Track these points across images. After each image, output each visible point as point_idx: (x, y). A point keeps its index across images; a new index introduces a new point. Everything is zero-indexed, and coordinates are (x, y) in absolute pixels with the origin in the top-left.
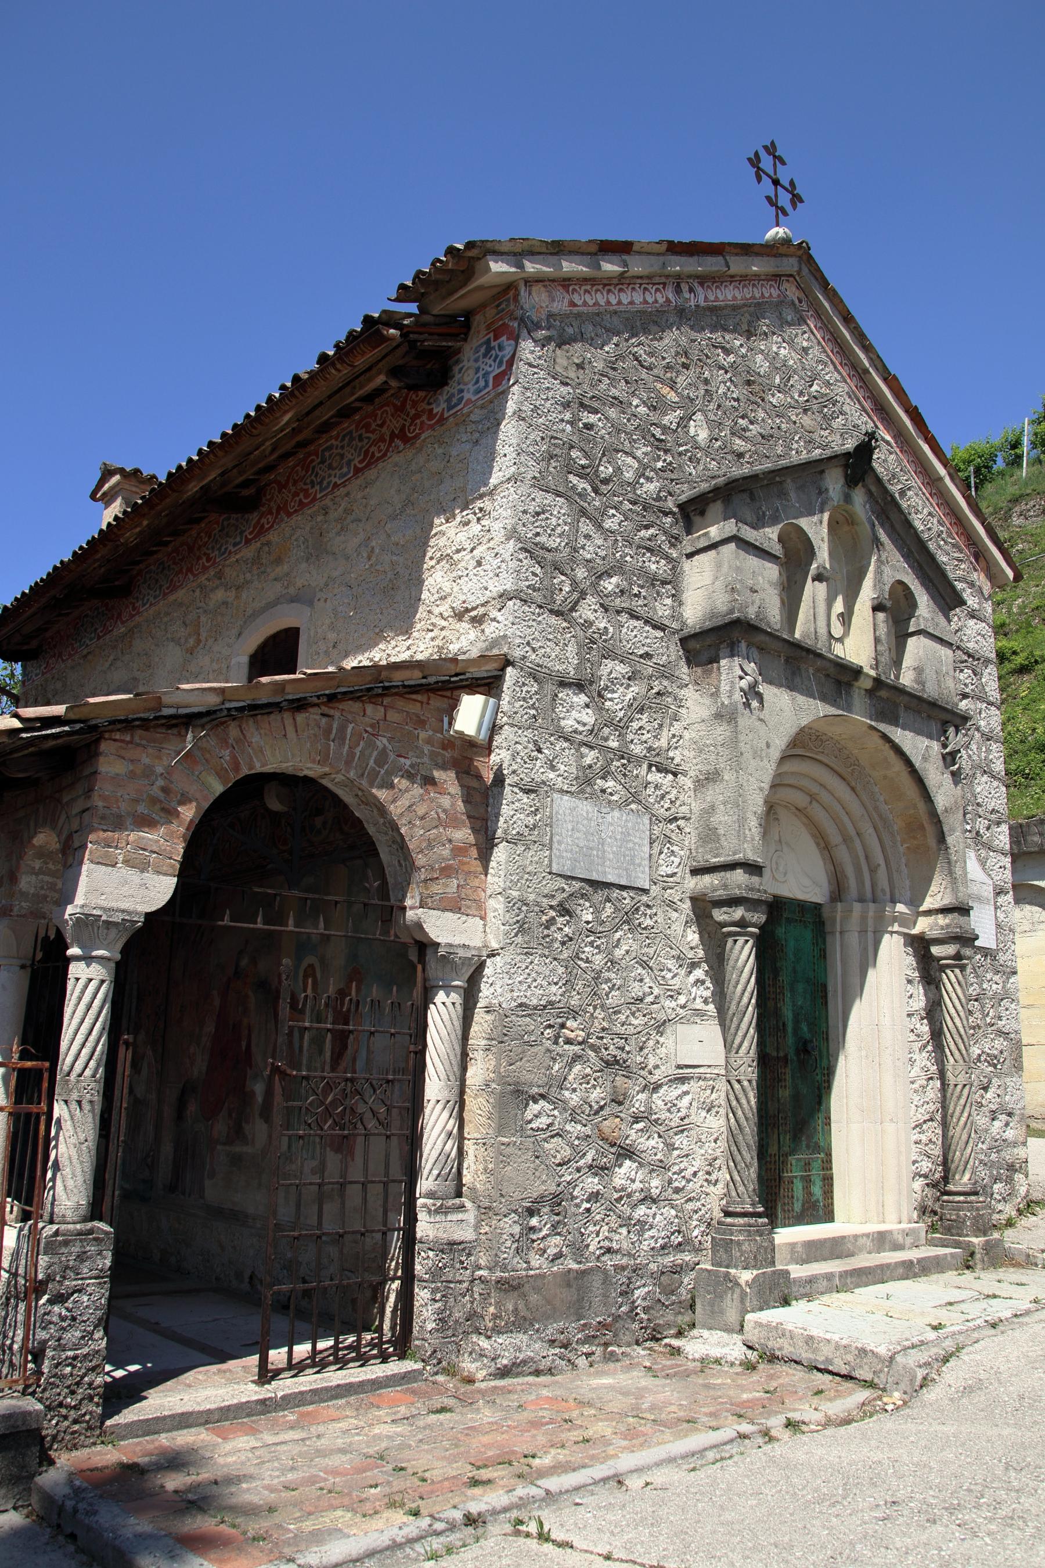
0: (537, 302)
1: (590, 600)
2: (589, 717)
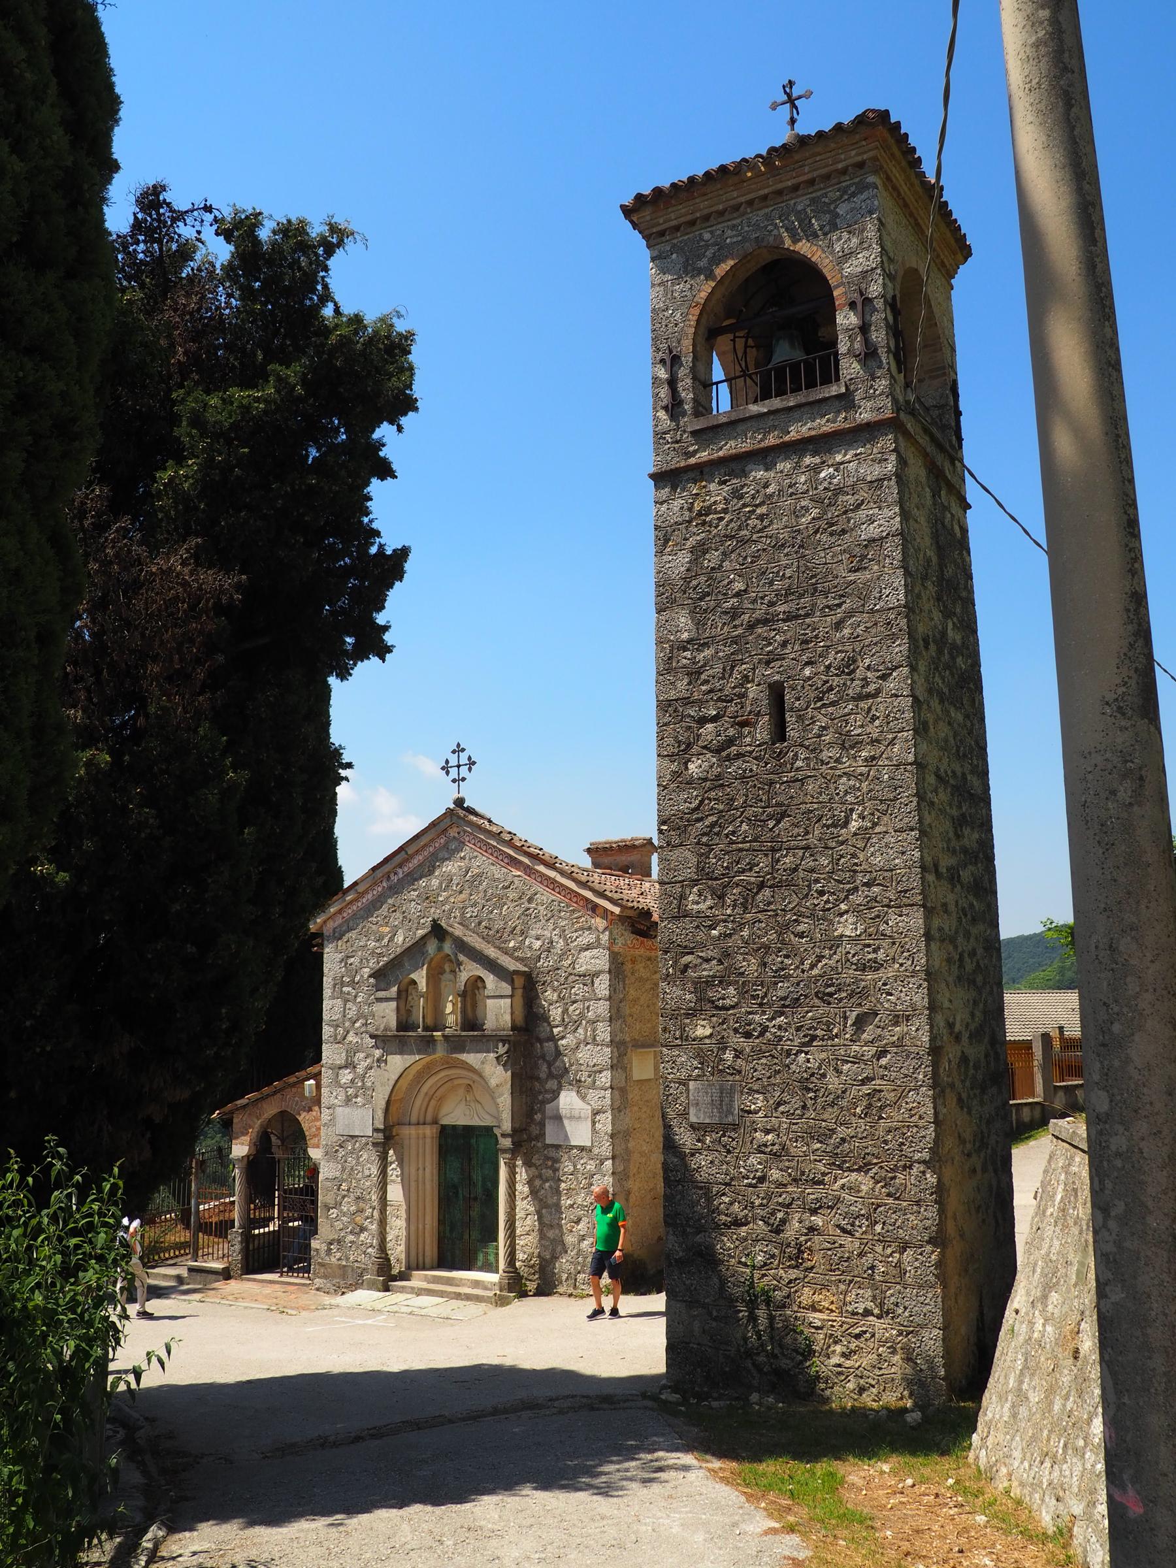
0: (328, 930)
1: (351, 1033)
2: (350, 1077)
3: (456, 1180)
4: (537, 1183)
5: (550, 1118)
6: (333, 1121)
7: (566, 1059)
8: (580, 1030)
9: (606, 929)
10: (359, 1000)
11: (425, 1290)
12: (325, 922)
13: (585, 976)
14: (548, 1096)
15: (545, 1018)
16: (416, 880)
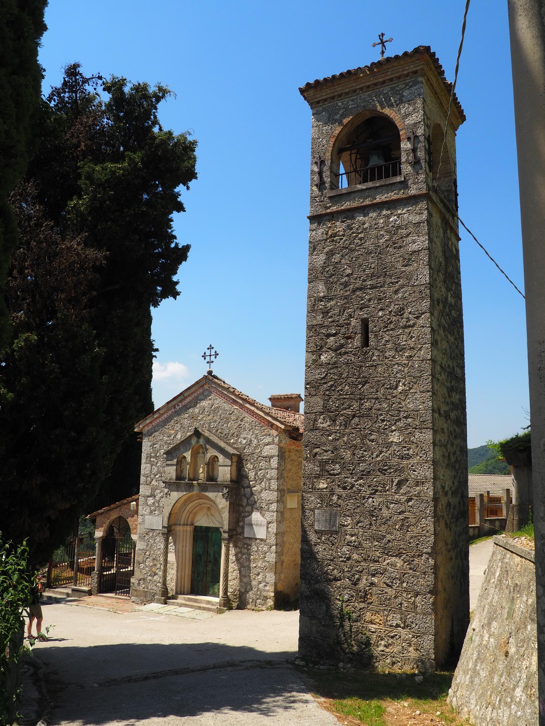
0: (145, 431)
1: (154, 480)
2: (152, 501)
3: (201, 552)
4: (240, 555)
5: (247, 525)
6: (144, 521)
7: (256, 497)
8: (263, 483)
9: (277, 435)
10: (158, 465)
11: (184, 604)
12: (144, 427)
13: (266, 457)
14: (246, 514)
15: (247, 477)
16: (189, 409)
